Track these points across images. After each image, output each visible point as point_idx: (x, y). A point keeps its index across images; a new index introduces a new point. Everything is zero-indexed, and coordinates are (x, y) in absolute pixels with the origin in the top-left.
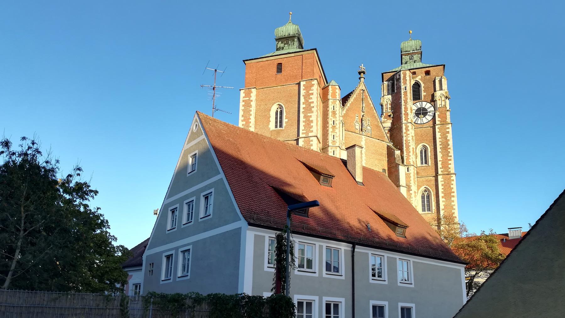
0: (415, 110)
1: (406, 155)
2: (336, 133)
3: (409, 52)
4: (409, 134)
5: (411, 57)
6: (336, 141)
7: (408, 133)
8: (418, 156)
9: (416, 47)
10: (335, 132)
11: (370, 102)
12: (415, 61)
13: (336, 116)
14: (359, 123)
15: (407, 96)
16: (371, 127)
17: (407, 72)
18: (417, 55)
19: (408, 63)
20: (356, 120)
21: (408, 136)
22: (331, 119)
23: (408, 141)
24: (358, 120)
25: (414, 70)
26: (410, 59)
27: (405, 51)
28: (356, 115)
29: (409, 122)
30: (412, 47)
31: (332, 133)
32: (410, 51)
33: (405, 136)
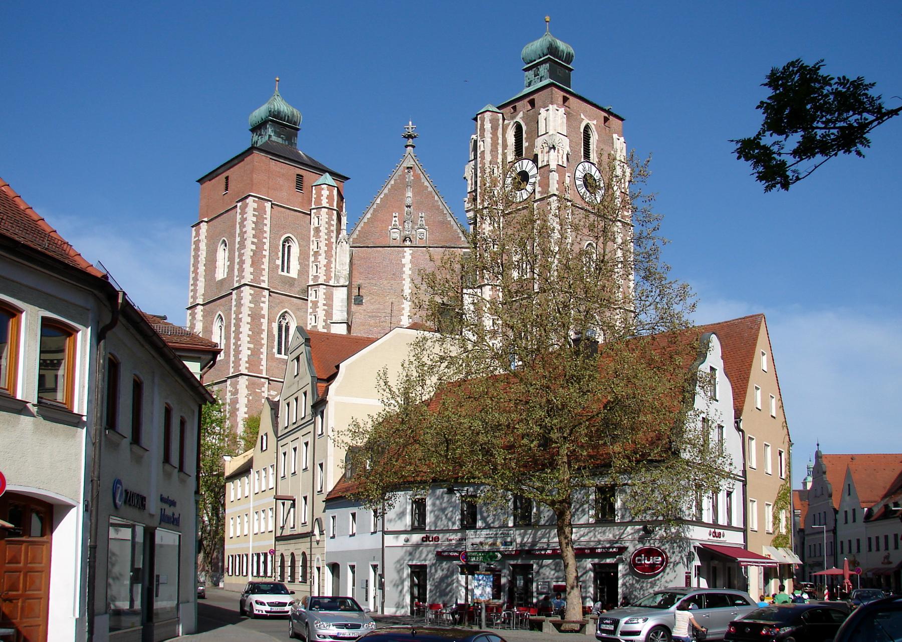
2: (319, 262)
6: (319, 275)
7: (483, 227)
11: (426, 184)
12: (541, 77)
13: (321, 234)
14: (400, 227)
15: (484, 159)
16: (427, 227)
18: (544, 65)
19: (532, 84)
20: (393, 223)
22: (313, 241)
24: (397, 223)
28: (394, 215)
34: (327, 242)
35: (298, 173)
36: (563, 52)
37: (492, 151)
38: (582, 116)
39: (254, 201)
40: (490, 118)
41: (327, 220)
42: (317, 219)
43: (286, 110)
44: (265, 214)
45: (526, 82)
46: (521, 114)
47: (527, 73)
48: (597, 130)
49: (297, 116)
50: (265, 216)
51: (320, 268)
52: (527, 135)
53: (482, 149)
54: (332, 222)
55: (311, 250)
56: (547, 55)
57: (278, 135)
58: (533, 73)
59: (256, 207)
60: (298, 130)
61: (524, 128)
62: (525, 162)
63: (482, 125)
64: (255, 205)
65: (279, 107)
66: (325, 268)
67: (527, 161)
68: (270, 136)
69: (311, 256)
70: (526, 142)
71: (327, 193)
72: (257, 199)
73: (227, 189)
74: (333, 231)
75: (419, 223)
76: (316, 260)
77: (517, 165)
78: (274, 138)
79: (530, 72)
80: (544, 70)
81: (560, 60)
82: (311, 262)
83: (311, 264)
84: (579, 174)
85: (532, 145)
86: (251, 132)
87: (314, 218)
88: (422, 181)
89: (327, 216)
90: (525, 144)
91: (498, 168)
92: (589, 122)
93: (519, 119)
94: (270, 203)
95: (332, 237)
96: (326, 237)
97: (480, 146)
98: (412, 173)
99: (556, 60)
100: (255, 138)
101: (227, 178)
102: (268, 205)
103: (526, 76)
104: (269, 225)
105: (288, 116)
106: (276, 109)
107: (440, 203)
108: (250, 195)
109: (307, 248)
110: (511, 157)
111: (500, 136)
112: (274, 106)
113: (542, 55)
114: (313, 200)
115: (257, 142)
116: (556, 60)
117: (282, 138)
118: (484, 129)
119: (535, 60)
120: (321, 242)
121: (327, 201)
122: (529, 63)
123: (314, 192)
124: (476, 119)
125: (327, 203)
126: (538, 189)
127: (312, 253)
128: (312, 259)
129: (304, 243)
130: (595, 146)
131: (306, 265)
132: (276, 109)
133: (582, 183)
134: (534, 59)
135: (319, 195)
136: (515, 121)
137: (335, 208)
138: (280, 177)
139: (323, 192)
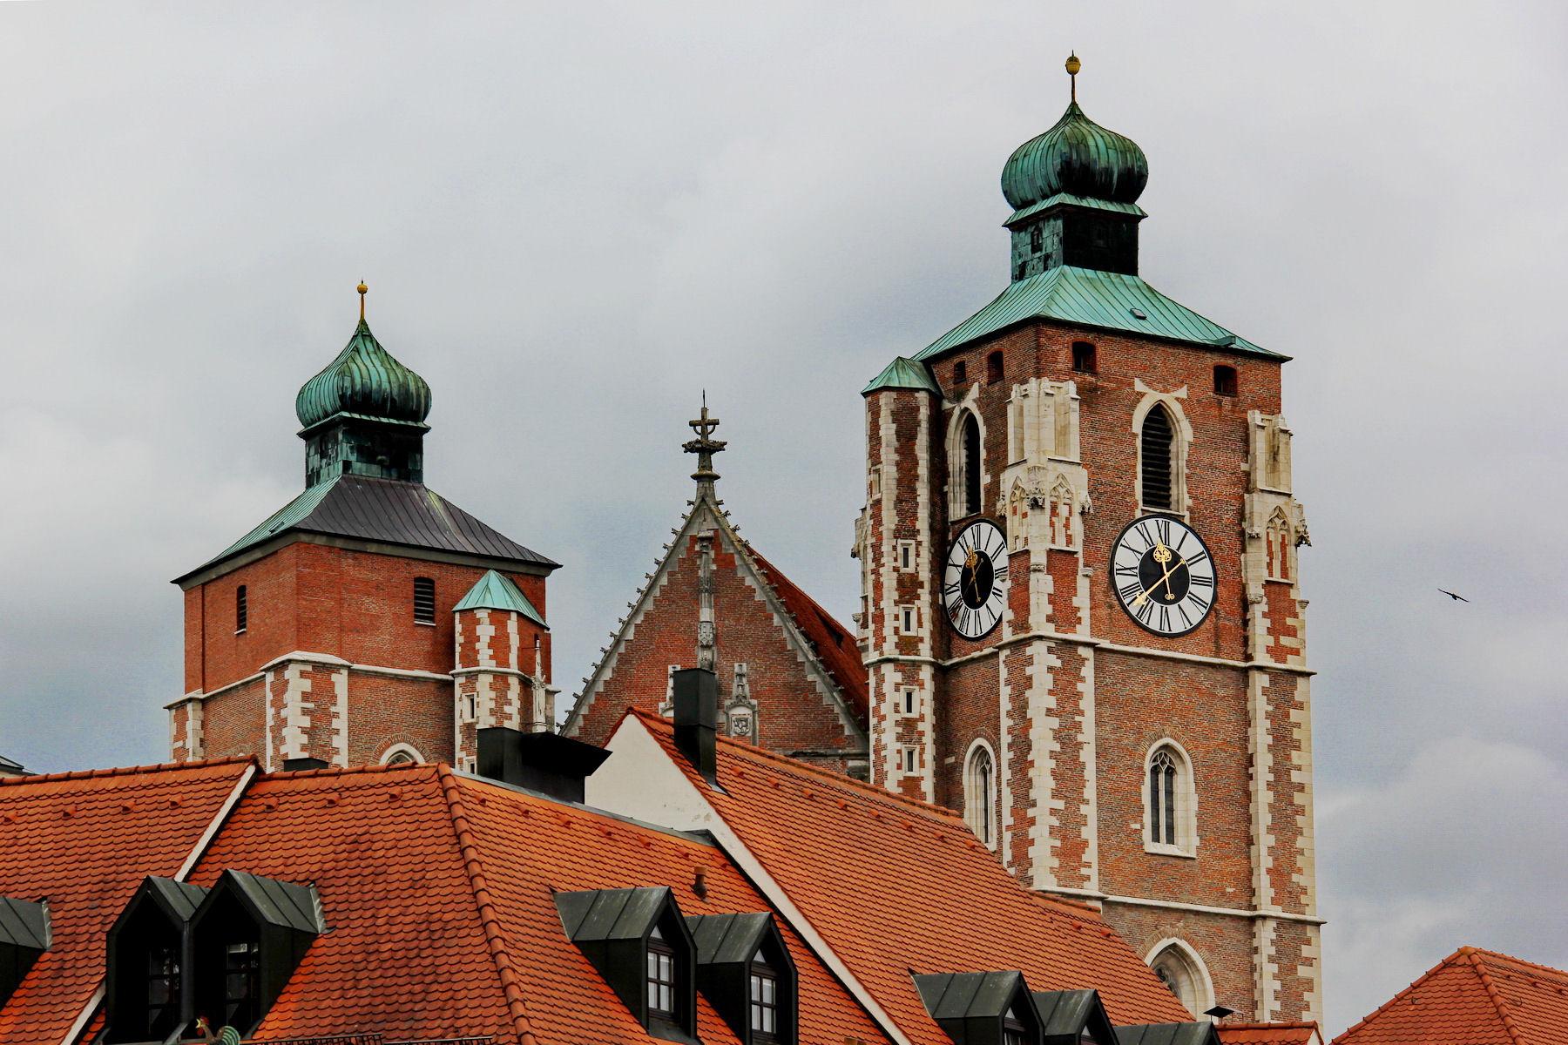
5: (1038, 235)
8: (967, 806)
9: (1046, 177)
12: (1047, 257)
18: (1052, 222)
19: (1028, 271)
33: (875, 730)
35: (417, 575)
36: (1108, 172)
38: (1139, 386)
39: (303, 674)
41: (492, 704)
42: (467, 702)
43: (385, 385)
44: (335, 704)
48: (1187, 415)
49: (419, 396)
50: (333, 709)
52: (988, 453)
54: (507, 709)
57: (367, 455)
58: (1028, 239)
59: (309, 689)
60: (427, 430)
64: (307, 685)
65: (366, 380)
68: (347, 465)
72: (309, 668)
73: (242, 621)
75: (735, 691)
78: (358, 467)
79: (1023, 234)
84: (1126, 558)
86: (303, 442)
87: (461, 699)
88: (740, 574)
89: (493, 694)
90: (985, 479)
91: (919, 544)
92: (1163, 397)
94: (345, 672)
98: (712, 554)
100: (315, 460)
101: (242, 591)
102: (340, 681)
104: (344, 732)
105: (393, 400)
106: (358, 387)
107: (785, 634)
108: (290, 661)
112: (353, 380)
113: (1047, 190)
114: (458, 649)
115: (318, 473)
117: (381, 463)
118: (879, 439)
119: (1033, 202)
121: (491, 652)
125: (491, 657)
130: (1183, 463)
132: (358, 387)
133: (1137, 579)
135: (471, 639)
138: (368, 594)
139: (480, 630)
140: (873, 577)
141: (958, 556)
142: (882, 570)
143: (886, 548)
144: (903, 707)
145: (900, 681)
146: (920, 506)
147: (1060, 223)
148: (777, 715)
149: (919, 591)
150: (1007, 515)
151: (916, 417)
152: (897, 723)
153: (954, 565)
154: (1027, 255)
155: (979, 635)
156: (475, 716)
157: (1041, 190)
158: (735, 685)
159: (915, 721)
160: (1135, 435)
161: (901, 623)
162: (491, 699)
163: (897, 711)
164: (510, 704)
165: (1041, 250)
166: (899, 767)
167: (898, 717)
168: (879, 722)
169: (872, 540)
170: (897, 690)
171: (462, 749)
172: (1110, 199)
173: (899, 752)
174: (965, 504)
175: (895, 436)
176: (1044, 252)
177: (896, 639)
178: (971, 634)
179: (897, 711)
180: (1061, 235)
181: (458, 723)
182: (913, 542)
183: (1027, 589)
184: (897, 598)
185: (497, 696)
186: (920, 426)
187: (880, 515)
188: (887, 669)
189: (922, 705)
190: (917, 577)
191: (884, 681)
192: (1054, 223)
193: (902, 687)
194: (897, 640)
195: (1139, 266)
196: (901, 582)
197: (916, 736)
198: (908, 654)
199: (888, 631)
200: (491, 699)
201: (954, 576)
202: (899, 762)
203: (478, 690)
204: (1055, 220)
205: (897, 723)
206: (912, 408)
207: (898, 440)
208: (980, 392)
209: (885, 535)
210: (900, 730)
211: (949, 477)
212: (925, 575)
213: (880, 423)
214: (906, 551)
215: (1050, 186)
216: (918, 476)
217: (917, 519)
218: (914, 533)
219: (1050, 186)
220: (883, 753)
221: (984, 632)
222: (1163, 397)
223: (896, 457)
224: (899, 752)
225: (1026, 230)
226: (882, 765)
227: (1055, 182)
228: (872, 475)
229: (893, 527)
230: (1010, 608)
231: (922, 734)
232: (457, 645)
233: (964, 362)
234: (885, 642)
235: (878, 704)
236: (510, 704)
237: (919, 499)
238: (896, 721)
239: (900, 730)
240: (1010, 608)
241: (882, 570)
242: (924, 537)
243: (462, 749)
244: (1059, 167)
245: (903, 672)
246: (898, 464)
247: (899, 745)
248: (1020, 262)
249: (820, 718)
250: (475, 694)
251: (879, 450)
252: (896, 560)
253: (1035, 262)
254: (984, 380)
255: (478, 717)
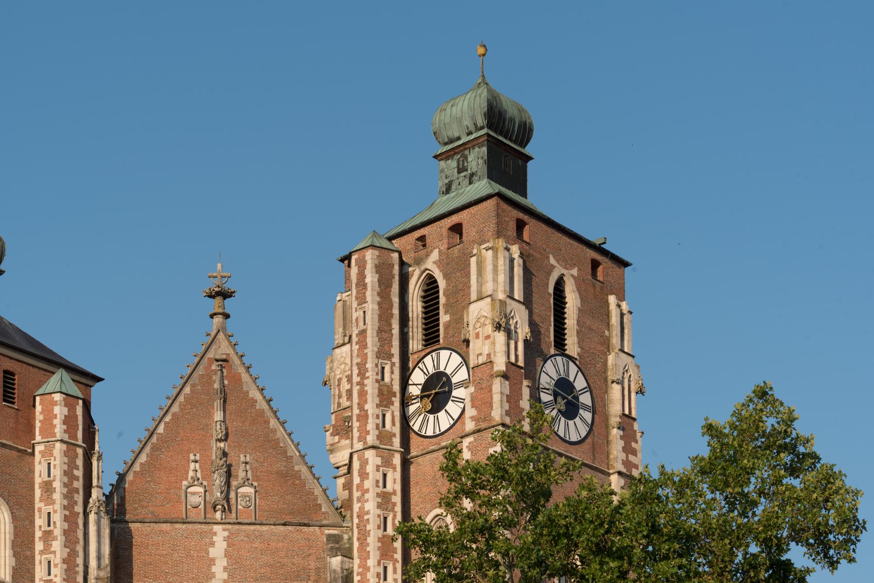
0: (420, 387)
1: (359, 567)
2: (54, 552)
3: (460, 142)
4: (367, 491)
5: (463, 161)
7: (365, 487)
9: (473, 118)
10: (52, 549)
12: (472, 175)
15: (365, 347)
17: (367, 254)
18: (477, 149)
19: (453, 187)
21: (367, 496)
22: (40, 510)
23: (366, 517)
25: (454, 219)
26: (459, 172)
27: (446, 140)
29: (370, 443)
30: (460, 121)
31: (44, 556)
32: (459, 138)
33: (359, 500)
34: (67, 513)
36: (512, 120)
37: (380, 331)
38: (552, 261)
40: (376, 262)
45: (441, 184)
46: (435, 255)
47: (442, 163)
51: (56, 565)
53: (361, 326)
54: (76, 472)
55: (37, 528)
56: (482, 128)
61: (442, 284)
62: (444, 354)
63: (362, 276)
66: (65, 566)
67: (449, 352)
69: (37, 539)
70: (446, 313)
71: (65, 411)
74: (77, 491)
76: (47, 550)
77: (428, 360)
79: (449, 162)
80: (477, 159)
81: (506, 137)
82: (37, 553)
83: (37, 557)
85: (458, 320)
91: (393, 364)
93: (432, 264)
95: (76, 503)
96: (65, 502)
97: (357, 320)
99: (501, 138)
103: (442, 171)
109: (27, 522)
110: (416, 343)
111: (396, 300)
113: (472, 128)
114: (38, 425)
116: (501, 138)
119: (459, 138)
120: (55, 512)
121: (65, 427)
122: (446, 144)
123: (38, 408)
124: (346, 259)
125: (65, 431)
126: (470, 412)
127: (38, 534)
128: (39, 546)
129: (22, 514)
131: (26, 558)
134: (456, 135)
136: (423, 268)
137: (80, 442)
140: (358, 387)
141: (418, 377)
142: (366, 382)
143: (369, 365)
144: (381, 484)
145: (380, 463)
146: (394, 337)
147: (485, 149)
148: (271, 494)
149: (393, 399)
150: (471, 339)
151: (391, 271)
152: (378, 495)
153: (414, 384)
154: (453, 176)
155: (438, 432)
156: (52, 475)
157: (468, 128)
158: (240, 471)
159: (391, 494)
160: (550, 294)
161: (380, 421)
162: (65, 463)
163: (378, 486)
164: (78, 469)
165: (467, 170)
166: (379, 527)
167: (380, 490)
168: (363, 495)
169: (356, 360)
170: (378, 470)
171: (41, 501)
172: (510, 140)
173: (379, 516)
174: (421, 342)
175: (377, 283)
176: (469, 172)
177: (377, 432)
178: (430, 433)
179: (378, 486)
180: (486, 157)
181: (38, 481)
182: (389, 362)
183: (491, 391)
184: (378, 402)
185: (69, 462)
186: (394, 278)
187: (365, 340)
188: (370, 454)
189: (395, 483)
190: (392, 388)
191: (367, 463)
192: (479, 150)
193: (381, 469)
194: (377, 433)
195: (528, 192)
196: (381, 394)
197: (390, 506)
198: (385, 445)
199: (371, 426)
200: (65, 463)
201: (414, 391)
202: (379, 523)
203: (54, 455)
204: (479, 147)
205: (378, 495)
206: (390, 264)
207: (380, 286)
208: (440, 255)
209: (370, 355)
210: (380, 500)
211: (408, 321)
212: (396, 388)
213: (366, 274)
214: (383, 368)
215: (475, 124)
216: (393, 315)
217: (392, 346)
218: (390, 356)
219: (475, 124)
220: (366, 517)
221: (442, 430)
222: (564, 271)
223: (378, 299)
224: (379, 516)
225: (452, 158)
226: (365, 526)
227: (481, 121)
228: (358, 312)
229: (376, 349)
230: (472, 407)
231: (394, 504)
232: (37, 422)
233: (425, 236)
234: (369, 434)
235: (362, 481)
236: (78, 469)
237: (393, 332)
238: (377, 493)
239: (380, 500)
240: (472, 407)
241: (366, 382)
242: (396, 359)
243: (41, 501)
244: (486, 109)
245: (382, 457)
246: (379, 304)
247: (379, 512)
248: (447, 181)
249: (304, 498)
250: (53, 458)
251: (365, 293)
252: (377, 374)
253: (460, 179)
254: (444, 247)
255: (55, 476)
